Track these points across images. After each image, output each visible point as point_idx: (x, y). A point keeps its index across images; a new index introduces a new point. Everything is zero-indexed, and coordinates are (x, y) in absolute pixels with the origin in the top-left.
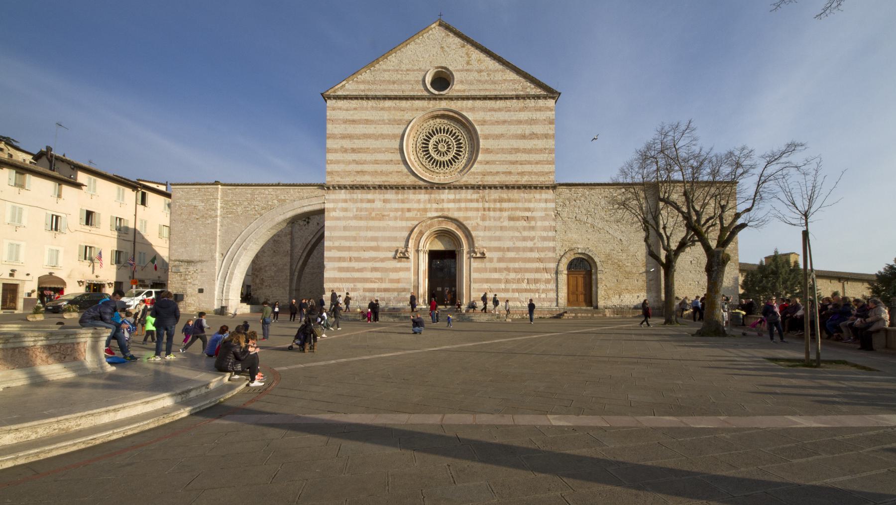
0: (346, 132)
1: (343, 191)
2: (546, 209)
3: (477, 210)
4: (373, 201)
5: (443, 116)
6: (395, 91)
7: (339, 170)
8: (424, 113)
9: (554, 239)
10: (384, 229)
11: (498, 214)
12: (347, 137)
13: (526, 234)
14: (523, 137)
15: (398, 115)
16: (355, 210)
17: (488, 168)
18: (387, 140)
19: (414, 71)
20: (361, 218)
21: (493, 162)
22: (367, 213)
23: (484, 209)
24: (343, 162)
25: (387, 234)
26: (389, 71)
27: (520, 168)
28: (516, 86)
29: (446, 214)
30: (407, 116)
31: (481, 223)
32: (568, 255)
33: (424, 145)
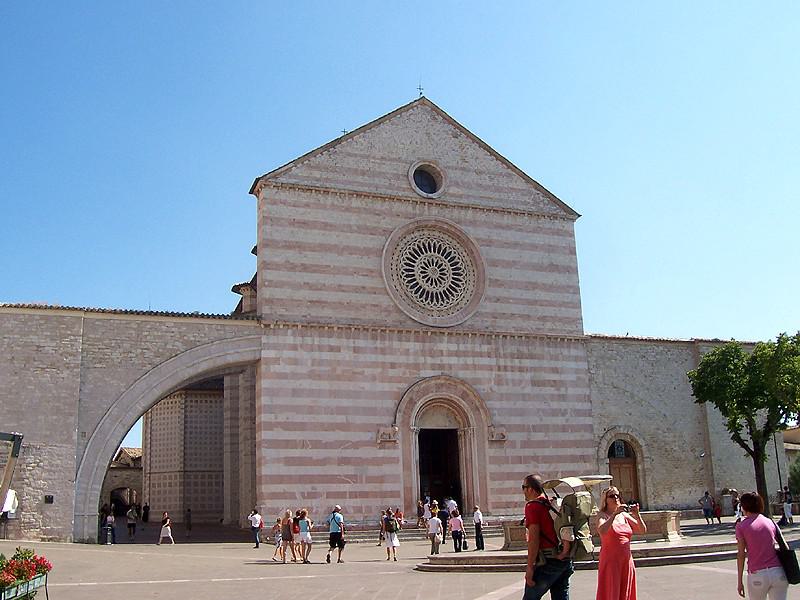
0: (293, 240)
1: (290, 331)
2: (577, 371)
3: (490, 368)
4: (338, 349)
5: (433, 228)
8: (408, 221)
9: (589, 414)
10: (356, 395)
11: (517, 375)
13: (555, 405)
14: (539, 268)
15: (371, 221)
17: (500, 308)
19: (391, 160)
20: (319, 376)
21: (506, 300)
23: (499, 369)
25: (362, 403)
26: (356, 155)
28: (526, 199)
29: (446, 372)
30: (385, 223)
31: (495, 388)
32: (608, 436)
33: (408, 268)
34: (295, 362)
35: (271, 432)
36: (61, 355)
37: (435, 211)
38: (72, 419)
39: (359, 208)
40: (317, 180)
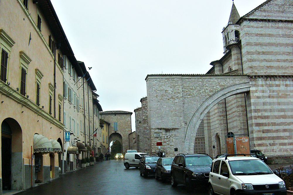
0: (257, 42)
6: (284, 17)
7: (256, 66)
12: (259, 45)
16: (269, 92)
18: (283, 47)
20: (273, 97)
22: (277, 93)
24: (258, 60)
34: (263, 92)
35: (256, 120)
36: (175, 93)
38: (181, 118)
39: (282, 27)
40: (265, 16)
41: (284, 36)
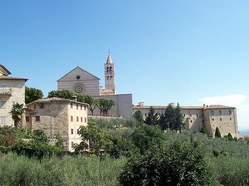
5: (79, 84)
14: (94, 87)
15: (70, 84)
27: (94, 93)
30: (72, 84)
37: (79, 82)
41: (69, 85)
